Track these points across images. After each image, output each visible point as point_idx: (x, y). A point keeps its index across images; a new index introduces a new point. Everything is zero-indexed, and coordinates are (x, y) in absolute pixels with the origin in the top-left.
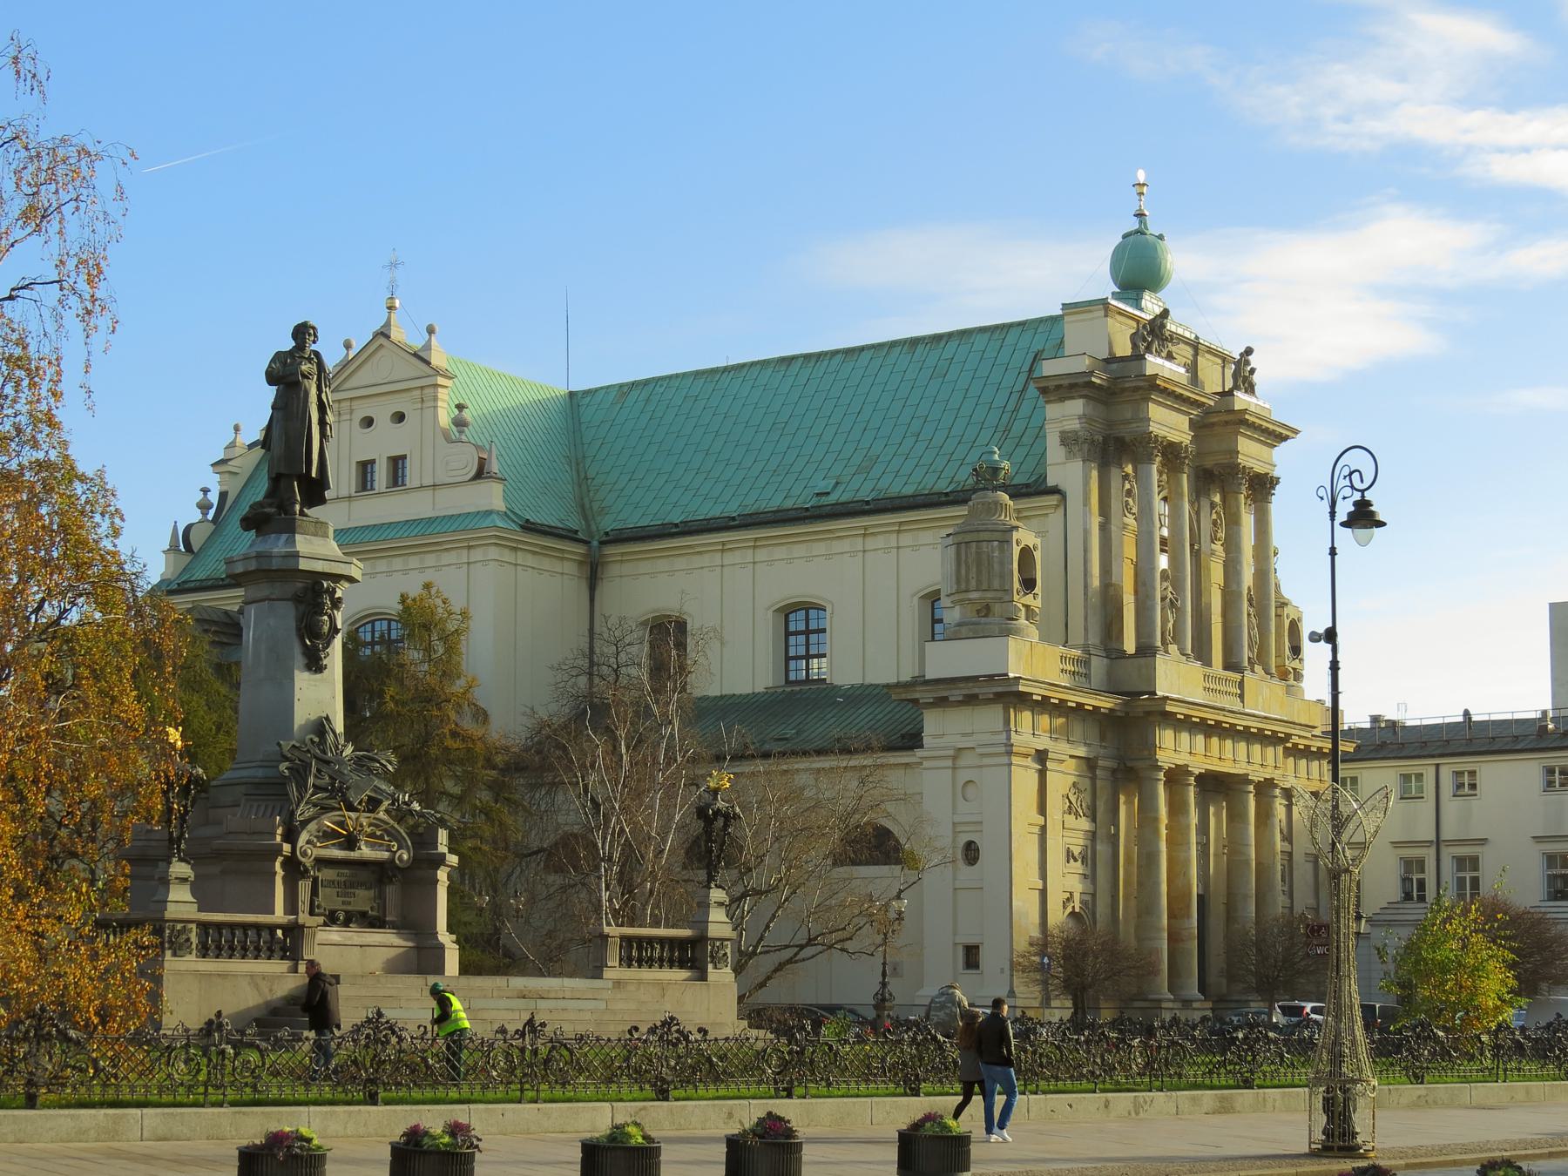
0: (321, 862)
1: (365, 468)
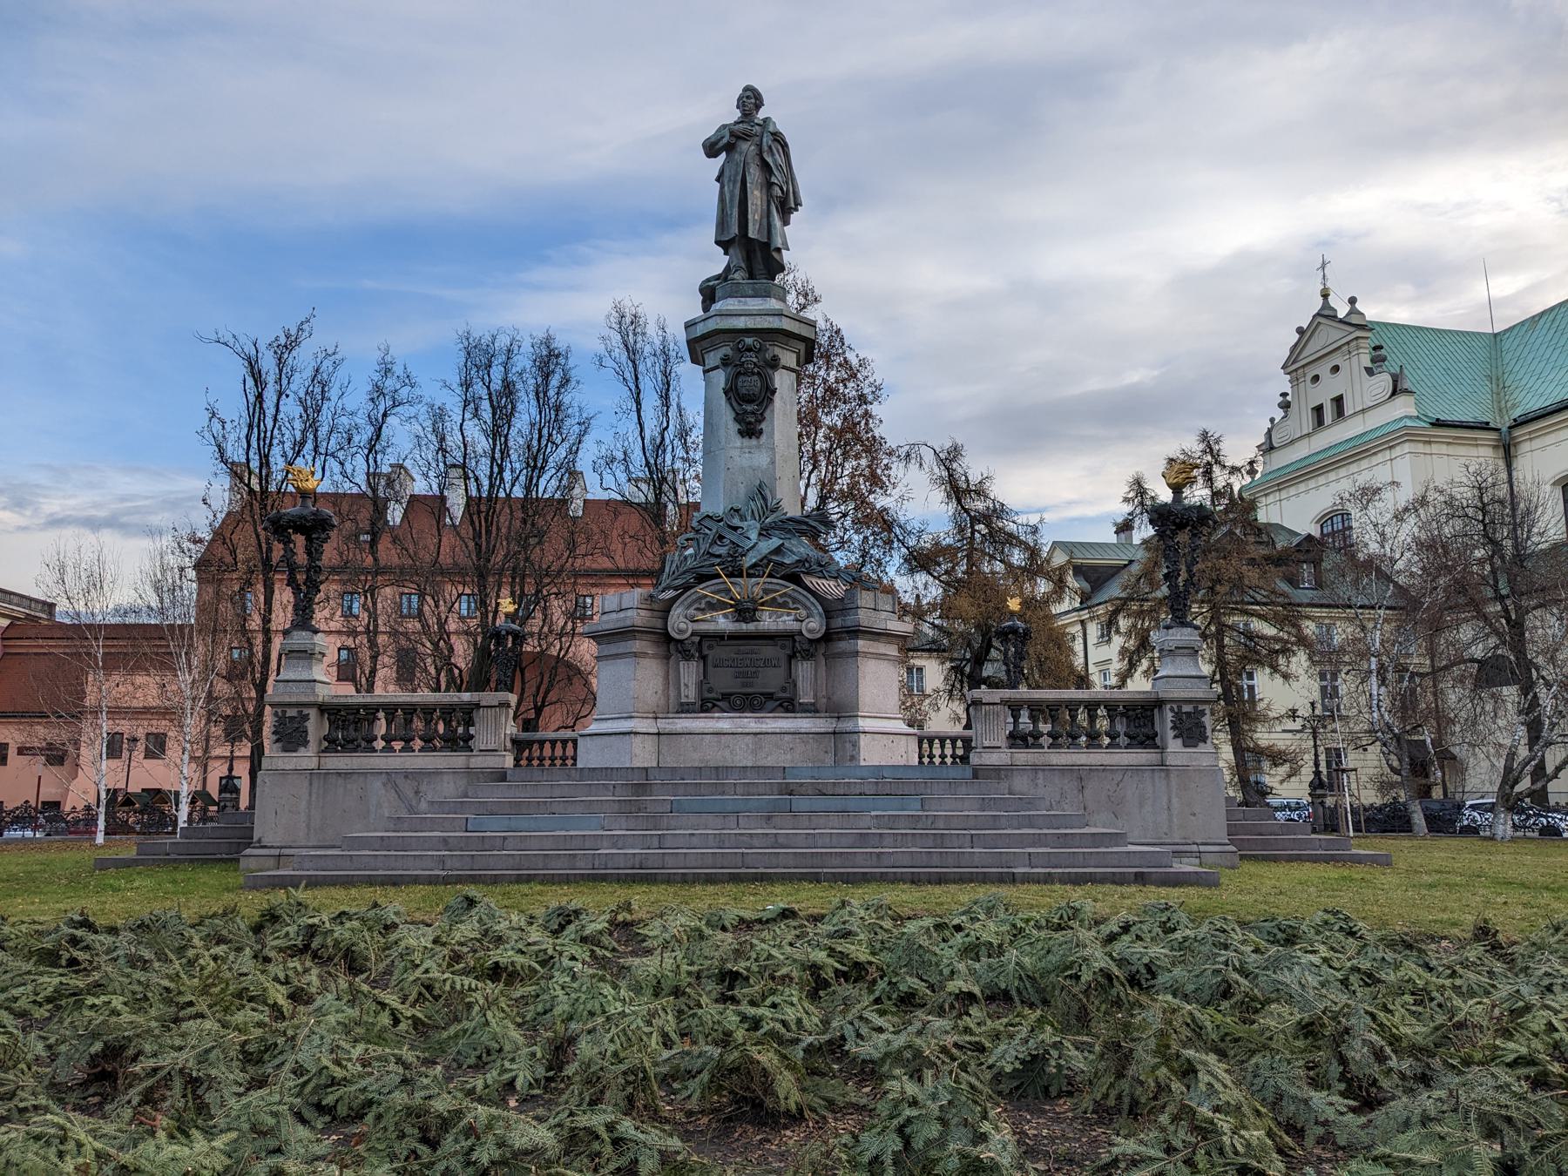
0: (705, 636)
1: (1319, 410)
